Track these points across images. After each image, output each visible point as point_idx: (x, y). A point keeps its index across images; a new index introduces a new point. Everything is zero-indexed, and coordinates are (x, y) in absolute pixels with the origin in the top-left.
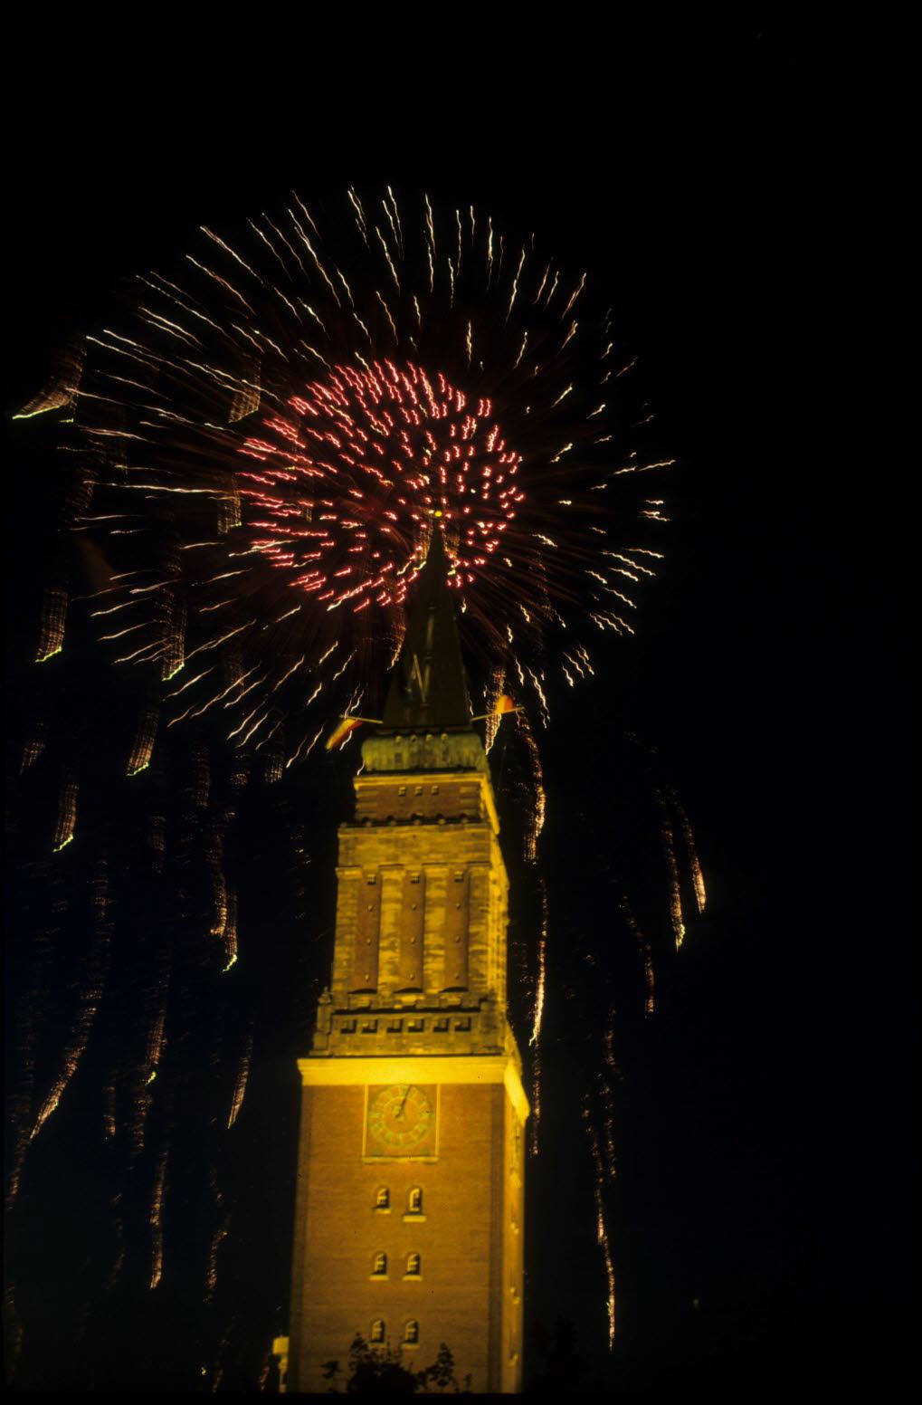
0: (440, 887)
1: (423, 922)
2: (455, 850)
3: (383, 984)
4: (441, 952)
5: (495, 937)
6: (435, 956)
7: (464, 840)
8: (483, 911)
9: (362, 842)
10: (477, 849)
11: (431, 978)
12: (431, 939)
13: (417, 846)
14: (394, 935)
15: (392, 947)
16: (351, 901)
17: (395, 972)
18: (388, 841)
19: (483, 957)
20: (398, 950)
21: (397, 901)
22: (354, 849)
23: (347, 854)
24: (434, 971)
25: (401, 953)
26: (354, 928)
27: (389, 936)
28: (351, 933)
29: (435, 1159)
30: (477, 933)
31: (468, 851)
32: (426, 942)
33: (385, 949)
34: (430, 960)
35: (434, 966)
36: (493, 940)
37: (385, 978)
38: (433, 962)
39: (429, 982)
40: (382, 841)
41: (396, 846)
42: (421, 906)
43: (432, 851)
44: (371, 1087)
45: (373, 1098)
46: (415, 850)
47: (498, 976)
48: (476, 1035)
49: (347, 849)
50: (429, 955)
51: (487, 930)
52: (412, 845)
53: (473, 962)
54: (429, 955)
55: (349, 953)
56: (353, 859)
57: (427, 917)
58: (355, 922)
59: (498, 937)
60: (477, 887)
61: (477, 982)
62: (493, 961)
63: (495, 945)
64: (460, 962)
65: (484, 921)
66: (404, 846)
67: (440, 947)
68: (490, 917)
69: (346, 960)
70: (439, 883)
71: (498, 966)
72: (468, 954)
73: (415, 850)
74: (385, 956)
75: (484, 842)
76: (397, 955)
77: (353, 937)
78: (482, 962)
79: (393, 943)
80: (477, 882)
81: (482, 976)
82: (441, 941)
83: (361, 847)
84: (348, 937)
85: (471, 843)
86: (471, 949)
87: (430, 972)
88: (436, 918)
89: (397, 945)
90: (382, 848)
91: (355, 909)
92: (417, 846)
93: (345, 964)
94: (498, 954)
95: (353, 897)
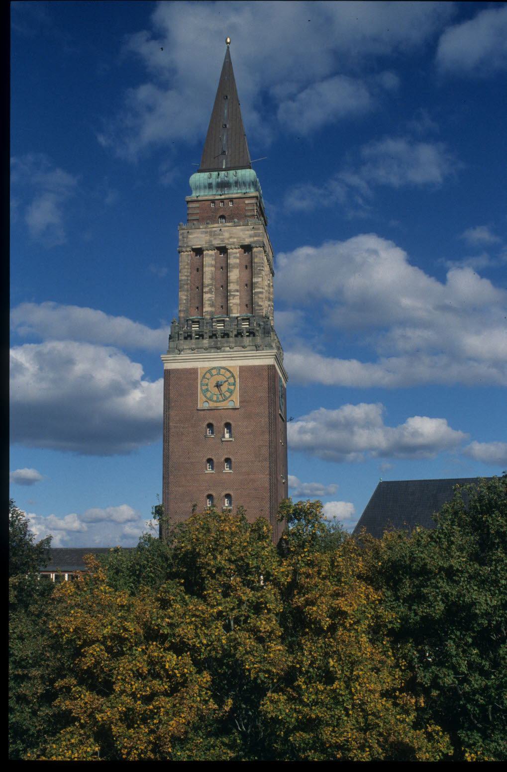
0: (235, 258)
1: (227, 277)
2: (244, 236)
3: (206, 312)
4: (238, 294)
5: (267, 284)
6: (234, 296)
7: (248, 230)
8: (259, 270)
9: (192, 233)
10: (255, 235)
11: (232, 308)
12: (232, 287)
13: (222, 235)
14: (212, 285)
15: (210, 292)
16: (186, 267)
17: (212, 305)
18: (206, 233)
19: (260, 295)
20: (213, 293)
21: (212, 266)
22: (187, 237)
23: (184, 241)
24: (234, 304)
25: (216, 295)
26: (189, 282)
27: (208, 285)
28: (187, 284)
29: (238, 406)
30: (257, 282)
31: (251, 236)
32: (229, 288)
33: (206, 293)
34: (231, 298)
35: (235, 301)
36: (266, 286)
37: (207, 308)
38: (233, 299)
39: (232, 310)
40: (202, 232)
41: (211, 235)
42: (225, 268)
43: (231, 237)
44: (200, 368)
45: (204, 377)
46: (221, 237)
47: (269, 306)
48: (258, 340)
49: (183, 237)
50: (231, 295)
51: (263, 280)
52: (219, 235)
53: (256, 299)
54: (231, 295)
55: (187, 296)
56: (187, 243)
57: (229, 275)
58: (189, 278)
59: (269, 284)
60: (257, 257)
61: (257, 310)
62: (266, 298)
63: (266, 288)
64: (249, 298)
65: (259, 276)
66: (214, 235)
67: (237, 291)
68: (264, 273)
69: (185, 299)
70: (235, 255)
71: (269, 300)
72: (252, 293)
73: (221, 237)
74: (206, 296)
75: (259, 231)
76: (214, 296)
77: (189, 286)
78: (259, 297)
79: (211, 289)
80: (256, 254)
81: (261, 306)
82: (237, 287)
83: (190, 236)
84: (186, 287)
85: (252, 232)
86: (254, 291)
87: (231, 305)
88: (234, 275)
89: (213, 290)
90: (203, 236)
91: (189, 270)
92: (222, 235)
93: (184, 301)
94: (269, 293)
95: (188, 264)
